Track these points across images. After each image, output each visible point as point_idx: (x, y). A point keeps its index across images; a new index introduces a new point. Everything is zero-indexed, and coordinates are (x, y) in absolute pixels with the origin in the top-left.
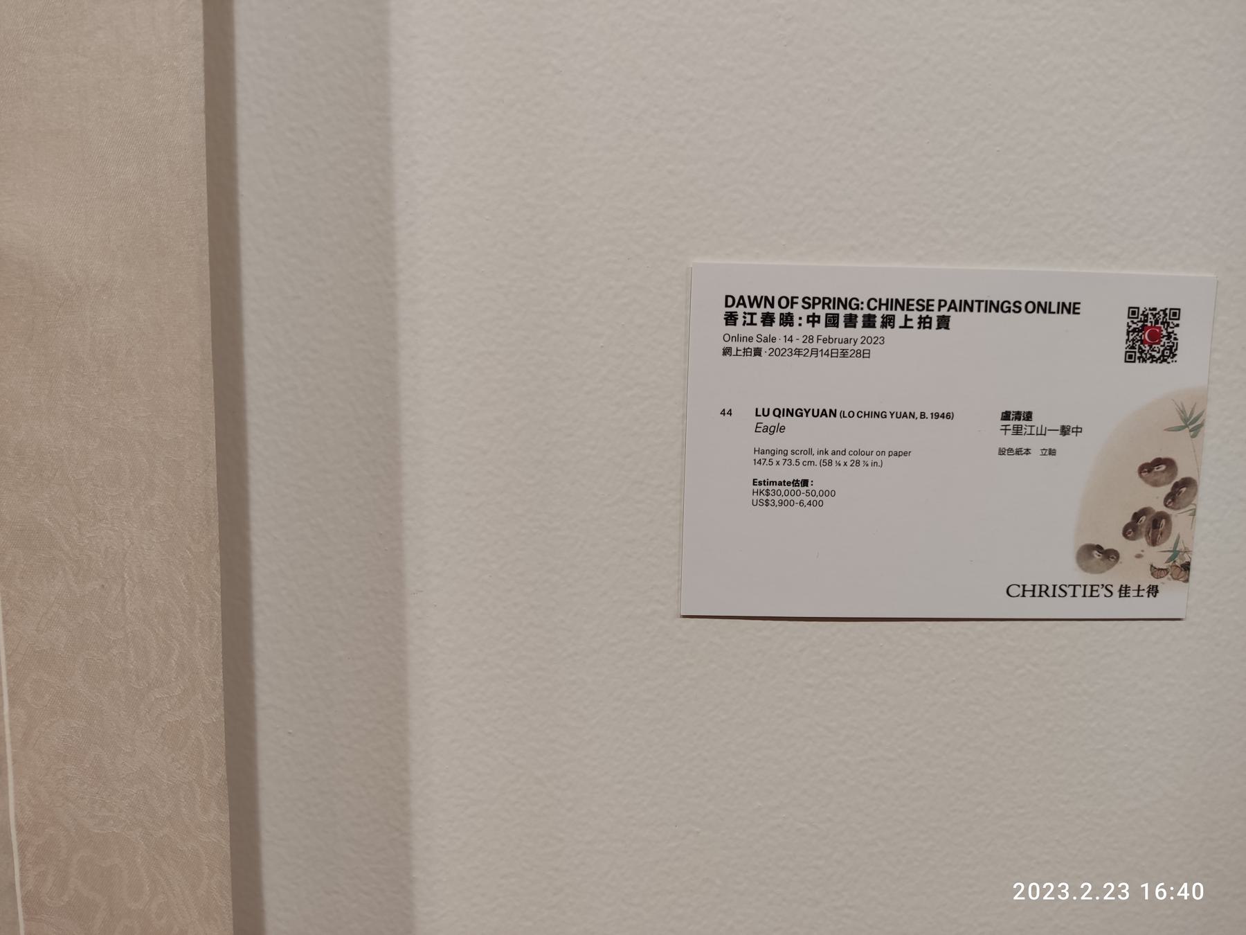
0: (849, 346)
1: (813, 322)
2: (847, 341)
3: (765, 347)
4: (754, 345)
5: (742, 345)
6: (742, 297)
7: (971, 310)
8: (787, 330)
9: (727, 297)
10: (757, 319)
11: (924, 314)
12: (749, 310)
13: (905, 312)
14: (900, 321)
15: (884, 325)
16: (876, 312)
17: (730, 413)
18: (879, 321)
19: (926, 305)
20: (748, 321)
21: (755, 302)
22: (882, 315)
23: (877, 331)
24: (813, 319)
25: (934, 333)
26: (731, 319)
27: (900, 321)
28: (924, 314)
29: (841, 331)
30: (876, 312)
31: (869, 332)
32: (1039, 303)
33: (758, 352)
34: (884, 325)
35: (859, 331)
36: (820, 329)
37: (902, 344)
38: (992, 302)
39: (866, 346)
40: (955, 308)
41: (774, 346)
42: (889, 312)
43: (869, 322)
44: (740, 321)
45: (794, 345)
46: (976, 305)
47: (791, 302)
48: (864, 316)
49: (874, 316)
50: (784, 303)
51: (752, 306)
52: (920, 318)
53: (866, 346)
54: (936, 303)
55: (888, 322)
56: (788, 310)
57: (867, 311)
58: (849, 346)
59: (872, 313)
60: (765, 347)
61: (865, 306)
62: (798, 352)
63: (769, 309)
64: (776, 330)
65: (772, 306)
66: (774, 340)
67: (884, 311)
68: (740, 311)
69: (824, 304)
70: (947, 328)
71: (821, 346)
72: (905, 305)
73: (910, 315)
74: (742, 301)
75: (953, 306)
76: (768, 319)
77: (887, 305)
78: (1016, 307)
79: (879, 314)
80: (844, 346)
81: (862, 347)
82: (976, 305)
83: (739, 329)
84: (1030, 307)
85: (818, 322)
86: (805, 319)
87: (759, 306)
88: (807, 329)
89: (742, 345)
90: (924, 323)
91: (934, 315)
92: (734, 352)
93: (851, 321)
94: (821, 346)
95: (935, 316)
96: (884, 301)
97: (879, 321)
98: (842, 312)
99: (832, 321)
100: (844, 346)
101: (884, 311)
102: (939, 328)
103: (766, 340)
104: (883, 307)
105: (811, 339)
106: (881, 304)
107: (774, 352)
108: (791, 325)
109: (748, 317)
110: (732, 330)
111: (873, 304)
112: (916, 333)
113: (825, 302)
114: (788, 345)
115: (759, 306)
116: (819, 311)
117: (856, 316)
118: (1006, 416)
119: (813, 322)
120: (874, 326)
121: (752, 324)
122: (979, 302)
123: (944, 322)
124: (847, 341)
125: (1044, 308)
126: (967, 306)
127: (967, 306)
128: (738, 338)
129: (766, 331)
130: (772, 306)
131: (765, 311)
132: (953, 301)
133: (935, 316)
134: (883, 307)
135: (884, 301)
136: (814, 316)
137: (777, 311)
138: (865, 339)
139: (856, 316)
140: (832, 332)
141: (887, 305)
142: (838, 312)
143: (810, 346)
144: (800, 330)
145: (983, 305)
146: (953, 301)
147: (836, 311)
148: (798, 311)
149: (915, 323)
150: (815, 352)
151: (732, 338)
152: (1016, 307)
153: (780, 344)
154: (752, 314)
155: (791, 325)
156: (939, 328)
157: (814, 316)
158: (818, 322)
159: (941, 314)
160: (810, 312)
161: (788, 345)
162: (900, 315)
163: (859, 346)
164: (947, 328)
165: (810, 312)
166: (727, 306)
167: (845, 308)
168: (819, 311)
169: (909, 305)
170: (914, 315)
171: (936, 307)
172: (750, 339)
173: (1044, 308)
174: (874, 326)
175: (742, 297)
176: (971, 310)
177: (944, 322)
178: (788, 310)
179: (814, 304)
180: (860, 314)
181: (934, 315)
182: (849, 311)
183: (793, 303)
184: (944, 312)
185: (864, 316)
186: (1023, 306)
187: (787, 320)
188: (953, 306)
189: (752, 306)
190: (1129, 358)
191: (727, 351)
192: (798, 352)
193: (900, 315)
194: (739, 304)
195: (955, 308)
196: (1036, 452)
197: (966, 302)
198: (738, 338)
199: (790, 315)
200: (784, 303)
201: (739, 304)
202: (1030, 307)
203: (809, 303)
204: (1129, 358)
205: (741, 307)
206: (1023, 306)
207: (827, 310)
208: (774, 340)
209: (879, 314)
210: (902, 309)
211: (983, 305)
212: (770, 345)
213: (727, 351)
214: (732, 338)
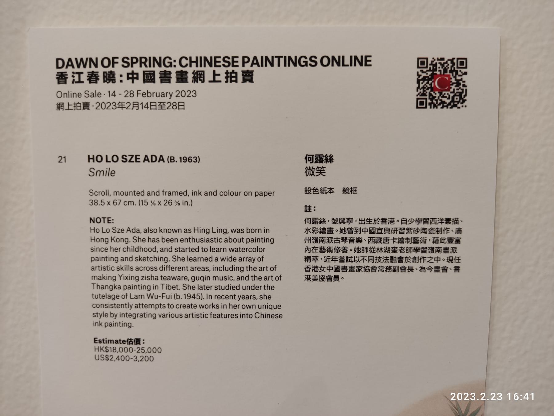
0: (166, 99)
1: (133, 79)
2: (164, 95)
3: (92, 101)
4: (82, 100)
5: (72, 100)
6: (70, 60)
7: (272, 65)
8: (110, 86)
9: (58, 60)
10: (84, 77)
11: (230, 69)
12: (76, 70)
13: (213, 68)
14: (209, 76)
15: (195, 80)
16: (187, 69)
18: (190, 76)
19: (231, 61)
20: (77, 79)
21: (81, 63)
22: (194, 71)
23: (190, 85)
24: (132, 77)
25: (240, 86)
26: (62, 78)
27: (209, 76)
28: (230, 69)
29: (158, 86)
30: (187, 69)
31: (182, 86)
32: (333, 58)
33: (86, 106)
34: (195, 80)
35: (173, 86)
36: (139, 84)
37: (211, 95)
38: (290, 58)
39: (181, 99)
40: (257, 64)
41: (100, 100)
42: (199, 69)
43: (182, 77)
44: (70, 80)
45: (117, 99)
46: (276, 60)
47: (113, 62)
48: (177, 72)
49: (186, 72)
50: (106, 63)
51: (79, 66)
52: (227, 73)
53: (181, 99)
54: (240, 60)
55: (199, 77)
56: (110, 69)
57: (179, 68)
58: (166, 99)
59: (184, 69)
60: (92, 101)
61: (177, 63)
62: (121, 105)
63: (93, 69)
64: (101, 86)
65: (96, 66)
66: (99, 95)
67: (194, 68)
68: (69, 71)
69: (141, 63)
70: (251, 81)
71: (140, 99)
72: (213, 62)
73: (218, 70)
74: (70, 63)
75: (255, 61)
76: (93, 78)
77: (196, 62)
78: (313, 61)
79: (190, 70)
80: (161, 99)
81: (177, 100)
82: (276, 60)
83: (69, 87)
84: (325, 61)
85: (137, 78)
86: (125, 76)
87: (85, 66)
89: (72, 100)
90: (230, 77)
91: (239, 70)
92: (66, 107)
93: (165, 77)
94: (140, 99)
95: (240, 71)
96: (194, 59)
97: (190, 76)
98: (157, 70)
99: (149, 78)
100: (161, 99)
101: (194, 68)
102: (244, 81)
103: (93, 95)
104: (194, 65)
105: (131, 94)
106: (191, 62)
107: (100, 105)
108: (114, 82)
109: (76, 76)
110: (63, 88)
111: (184, 62)
112: (224, 87)
113: (142, 61)
114: (112, 99)
115: (85, 66)
116: (137, 68)
117: (170, 73)
118: (309, 158)
119: (133, 79)
120: (186, 81)
121: (80, 82)
122: (279, 58)
123: (248, 77)
124: (164, 95)
125: (338, 61)
126: (268, 61)
127: (268, 61)
128: (69, 95)
129: (92, 88)
130: (96, 66)
131: (91, 70)
132: (255, 58)
133: (240, 71)
134: (194, 65)
135: (194, 59)
136: (133, 73)
137: (100, 70)
138: (179, 93)
139: (170, 73)
140: (149, 87)
141: (196, 62)
142: (154, 70)
143: (131, 100)
144: (122, 86)
145: (282, 60)
146: (255, 58)
147: (152, 69)
148: (119, 70)
149: (222, 78)
150: (136, 105)
151: (63, 95)
152: (313, 61)
153: (105, 98)
154: (79, 74)
155: (114, 82)
156: (244, 81)
157: (133, 73)
158: (137, 78)
159: (245, 69)
160: (129, 70)
161: (112, 99)
162: (208, 71)
163: (174, 99)
164: (251, 81)
165: (129, 70)
166: (58, 67)
167: (160, 65)
168: (137, 68)
169: (216, 62)
170: (221, 71)
171: (240, 63)
172: (79, 95)
173: (338, 61)
174: (186, 81)
175: (70, 60)
176: (272, 65)
177: (248, 77)
178: (110, 69)
179: (133, 63)
180: (173, 70)
181: (239, 70)
182: (163, 68)
183: (114, 63)
184: (248, 67)
185: (177, 72)
186: (318, 60)
187: (110, 77)
188: (255, 61)
189: (79, 66)
190: (420, 104)
191: (60, 106)
192: (121, 105)
193: (208, 71)
194: (68, 65)
195: (257, 64)
197: (267, 58)
199: (112, 74)
200: (106, 63)
201: (68, 65)
202: (325, 61)
203: (128, 62)
204: (420, 104)
205: (70, 68)
206: (318, 60)
207: (144, 68)
208: (99, 95)
209: (190, 70)
210: (211, 65)
211: (282, 60)
212: (96, 99)
213: (60, 106)
214: (63, 95)
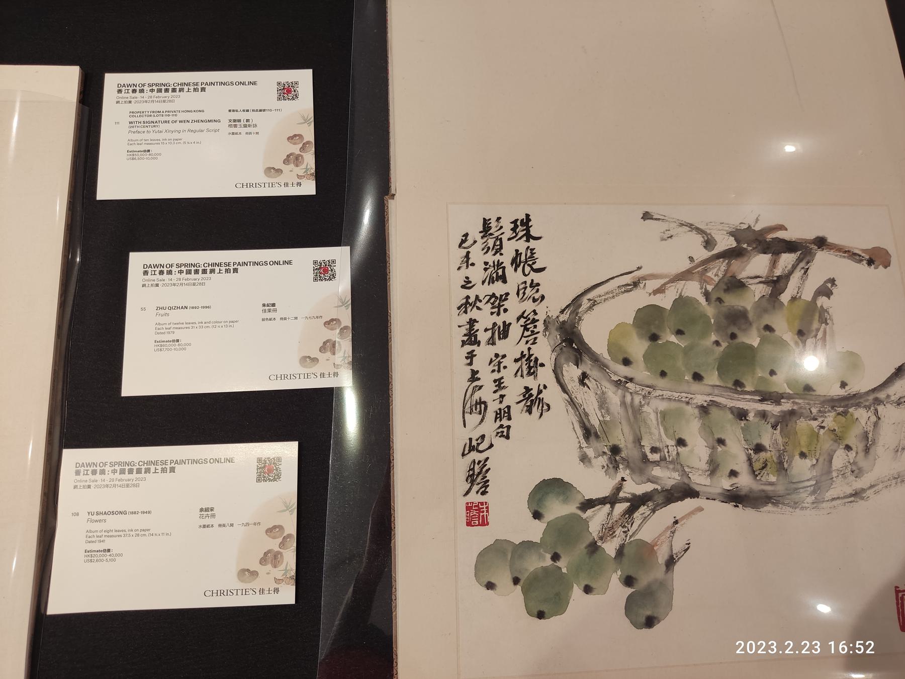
3: (92, 484)
4: (88, 483)
5: (82, 484)
14: (153, 470)
15: (145, 472)
17: (78, 514)
18: (143, 471)
19: (165, 463)
21: (89, 465)
23: (143, 475)
25: (168, 475)
29: (127, 476)
31: (139, 476)
33: (89, 487)
34: (145, 472)
35: (135, 475)
43: (139, 471)
44: (82, 473)
45: (105, 483)
55: (147, 471)
60: (92, 484)
74: (83, 465)
75: (176, 462)
83: (81, 477)
88: (112, 476)
89: (82, 484)
94: (117, 482)
97: (143, 471)
98: (127, 468)
99: (122, 472)
110: (78, 478)
112: (160, 475)
113: (119, 464)
128: (81, 481)
137: (98, 468)
149: (159, 471)
150: (115, 486)
153: (99, 483)
162: (153, 468)
163: (134, 482)
170: (159, 467)
181: (168, 467)
184: (173, 465)
188: (176, 462)
191: (75, 487)
193: (153, 468)
196: (216, 525)
198: (81, 481)
213: (75, 487)
